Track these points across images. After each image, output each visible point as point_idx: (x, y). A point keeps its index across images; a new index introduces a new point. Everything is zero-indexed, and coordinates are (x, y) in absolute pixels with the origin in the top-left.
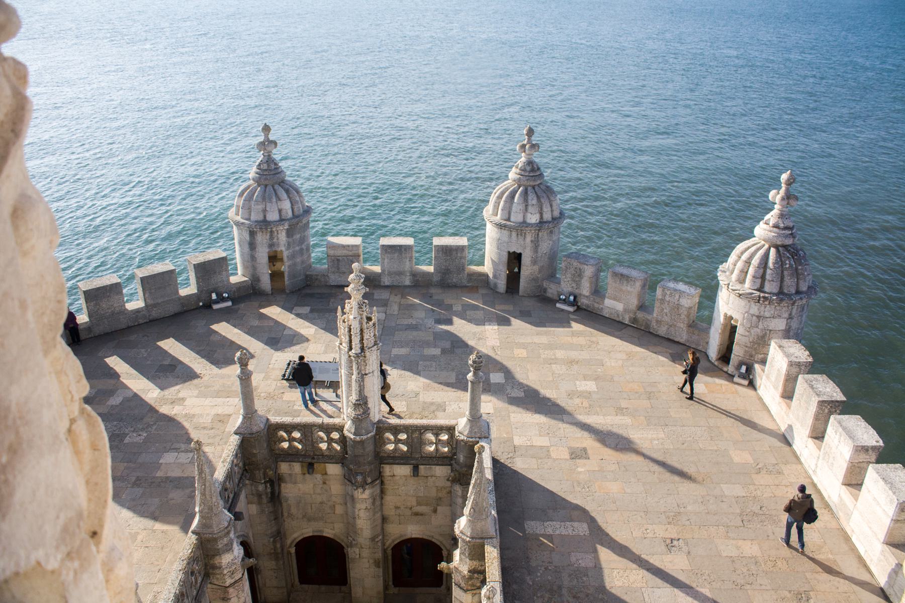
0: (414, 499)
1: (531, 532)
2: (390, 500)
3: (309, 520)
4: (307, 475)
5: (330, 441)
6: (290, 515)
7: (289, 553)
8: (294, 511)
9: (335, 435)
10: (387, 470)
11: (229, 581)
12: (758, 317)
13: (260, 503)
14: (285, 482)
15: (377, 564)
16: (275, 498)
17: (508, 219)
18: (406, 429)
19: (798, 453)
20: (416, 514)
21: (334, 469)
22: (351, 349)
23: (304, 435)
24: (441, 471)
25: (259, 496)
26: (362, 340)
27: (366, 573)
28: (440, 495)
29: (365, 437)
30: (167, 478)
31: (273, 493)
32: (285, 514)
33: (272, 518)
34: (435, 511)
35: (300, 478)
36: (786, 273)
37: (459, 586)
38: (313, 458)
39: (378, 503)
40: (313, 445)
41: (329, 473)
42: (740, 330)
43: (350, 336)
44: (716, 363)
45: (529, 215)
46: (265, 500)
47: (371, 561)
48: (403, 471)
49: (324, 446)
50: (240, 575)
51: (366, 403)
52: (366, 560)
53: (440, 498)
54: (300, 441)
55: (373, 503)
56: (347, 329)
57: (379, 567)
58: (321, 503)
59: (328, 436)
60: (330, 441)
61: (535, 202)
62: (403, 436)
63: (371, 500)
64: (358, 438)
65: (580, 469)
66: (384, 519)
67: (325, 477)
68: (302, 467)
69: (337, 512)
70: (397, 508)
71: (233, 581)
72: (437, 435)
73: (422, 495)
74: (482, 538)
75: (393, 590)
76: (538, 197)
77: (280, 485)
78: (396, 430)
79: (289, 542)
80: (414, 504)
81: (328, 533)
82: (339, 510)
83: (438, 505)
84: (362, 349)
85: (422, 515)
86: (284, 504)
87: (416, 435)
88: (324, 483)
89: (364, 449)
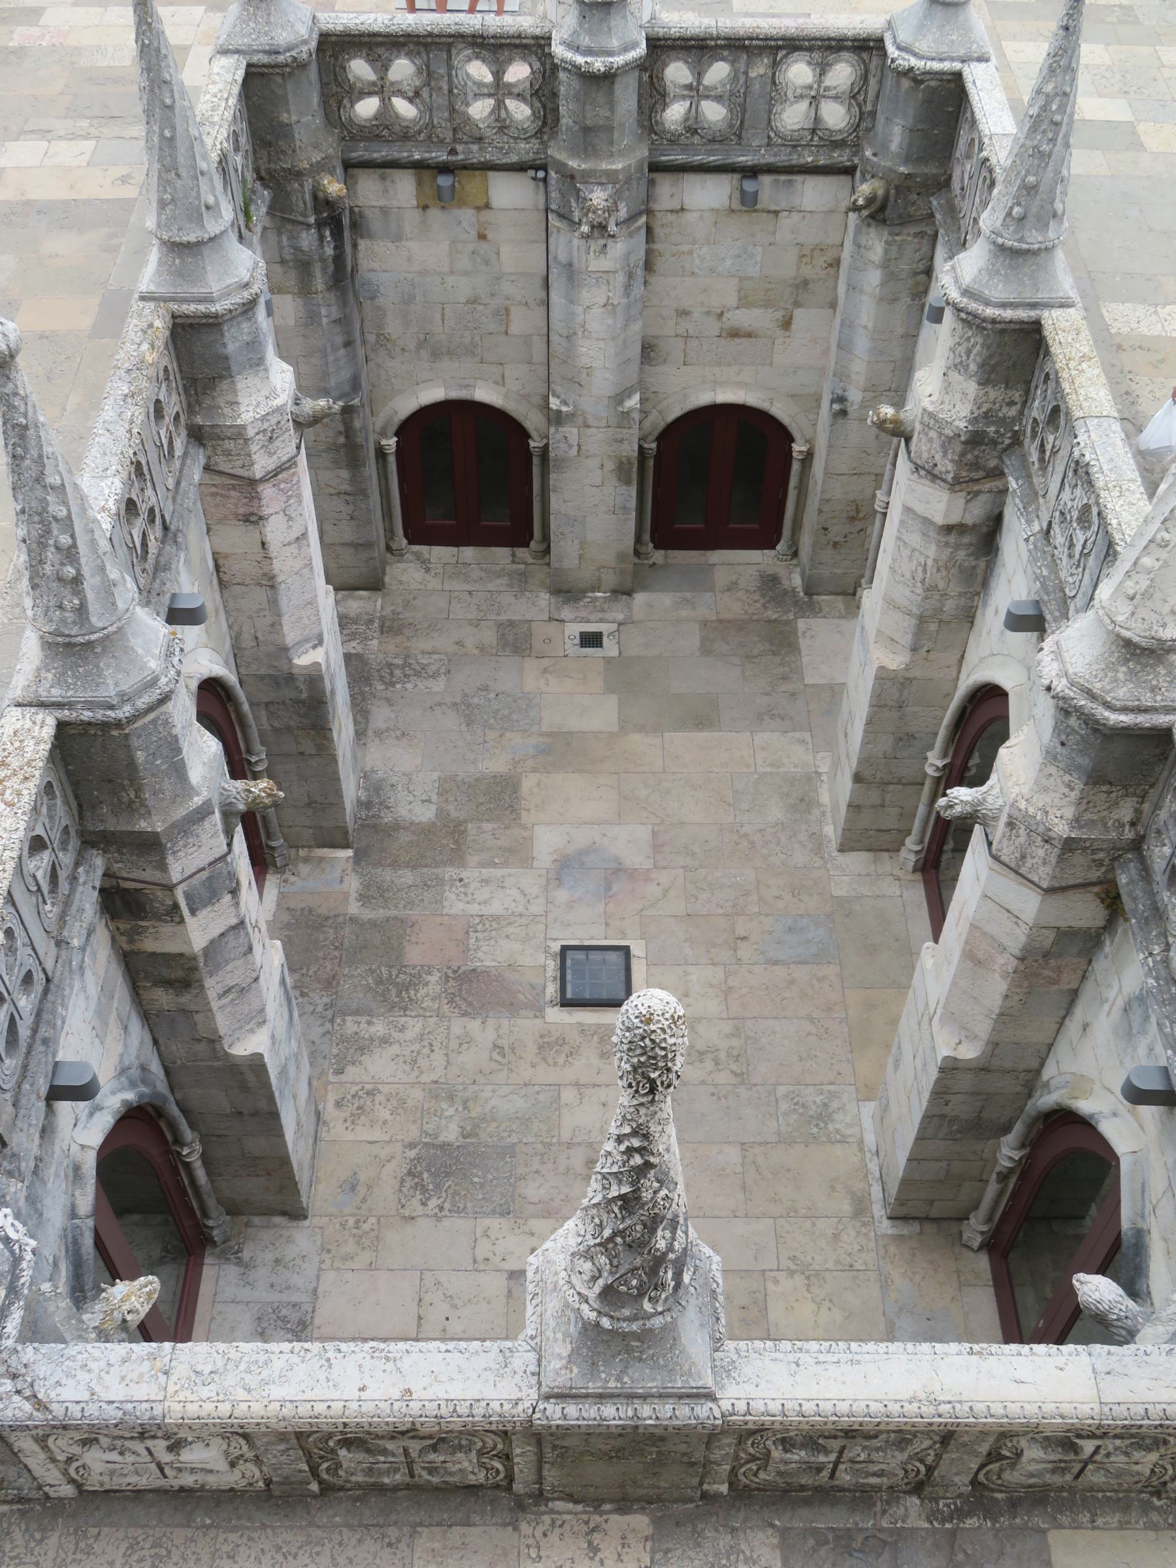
0: (733, 284)
1: (1125, 330)
2: (674, 288)
3: (436, 355)
4: (434, 213)
5: (499, 90)
6: (383, 340)
7: (381, 453)
8: (393, 327)
9: (519, 72)
10: (667, 191)
11: (261, 464)
13: (305, 290)
14: (370, 236)
15: (622, 470)
16: (342, 275)
18: (738, 46)
20: (734, 334)
21: (510, 194)
23: (428, 74)
24: (815, 194)
25: (303, 266)
27: (592, 502)
28: (808, 272)
29: (619, 60)
30: (28, 203)
31: (339, 259)
32: (371, 338)
33: (339, 340)
34: (787, 324)
35: (412, 218)
37: (933, 475)
38: (453, 152)
39: (638, 290)
40: (452, 110)
46: (319, 283)
47: (610, 466)
48: (708, 195)
49: (480, 110)
50: (292, 449)
52: (593, 463)
53: (806, 283)
54: (414, 97)
55: (628, 288)
57: (628, 483)
58: (473, 301)
59: (498, 74)
60: (499, 90)
62: (718, 72)
63: (620, 278)
64: (598, 64)
66: (649, 351)
67: (485, 216)
68: (420, 183)
69: (514, 329)
70: (683, 313)
71: (271, 463)
72: (822, 69)
73: (753, 271)
74: (1033, 306)
75: (658, 556)
77: (355, 246)
78: (699, 48)
79: (379, 422)
80: (732, 300)
81: (485, 394)
83: (797, 304)
85: (749, 335)
86: (367, 306)
87: (760, 68)
88: (482, 237)
89: (611, 104)
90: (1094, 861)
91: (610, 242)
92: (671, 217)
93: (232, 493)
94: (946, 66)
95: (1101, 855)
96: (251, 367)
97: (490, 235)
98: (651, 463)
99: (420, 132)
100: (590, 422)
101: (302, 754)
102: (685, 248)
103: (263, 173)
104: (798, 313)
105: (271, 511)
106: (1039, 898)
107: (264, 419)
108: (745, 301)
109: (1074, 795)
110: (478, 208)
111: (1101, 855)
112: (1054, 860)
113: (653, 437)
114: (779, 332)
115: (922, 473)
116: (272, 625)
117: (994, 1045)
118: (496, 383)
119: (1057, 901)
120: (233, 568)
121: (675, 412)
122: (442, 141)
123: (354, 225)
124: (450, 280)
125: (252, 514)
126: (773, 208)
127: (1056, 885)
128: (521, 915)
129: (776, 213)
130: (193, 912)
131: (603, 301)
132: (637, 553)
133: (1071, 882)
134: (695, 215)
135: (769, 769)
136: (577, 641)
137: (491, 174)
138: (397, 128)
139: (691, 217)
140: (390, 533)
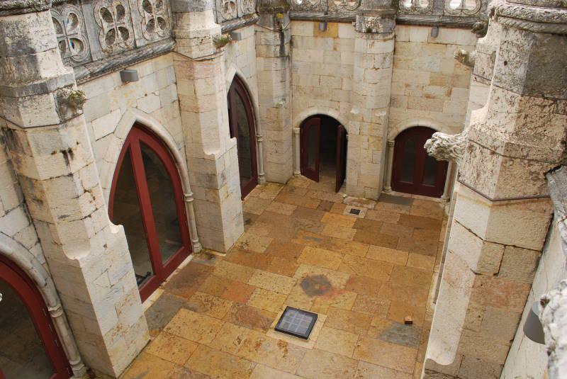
4: (319, 39)
10: (403, 32)
11: (196, 53)
20: (428, 97)
21: (344, 30)
27: (366, 160)
34: (449, 93)
41: (340, 36)
48: (419, 35)
53: (458, 76)
66: (393, 101)
67: (337, 41)
70: (407, 85)
80: (427, 82)
82: (345, 87)
85: (434, 98)
88: (335, 49)
90: (531, 173)
91: (376, 41)
92: (404, 44)
93: (185, 65)
95: (536, 167)
96: (197, 11)
97: (338, 49)
98: (392, 149)
99: (316, 7)
100: (365, 120)
101: (208, 201)
102: (410, 58)
103: (258, 11)
104: (454, 89)
105: (199, 76)
106: (489, 209)
107: (198, 32)
108: (433, 83)
109: (514, 109)
110: (334, 38)
111: (536, 167)
112: (498, 169)
113: (393, 138)
114: (446, 97)
115: (478, 79)
116: (198, 133)
117: (462, 358)
118: (336, 109)
119: (504, 214)
120: (185, 102)
121: (402, 128)
122: (323, 10)
123: (291, 43)
124: (323, 66)
125: (191, 76)
126: (445, 42)
127: (502, 197)
128: (278, 293)
129: (446, 44)
130: (39, 152)
131: (372, 67)
132: (384, 189)
133: (513, 194)
134: (414, 44)
135: (412, 266)
136: (349, 211)
137: (340, 24)
138: (309, 5)
139: (412, 45)
140: (294, 167)
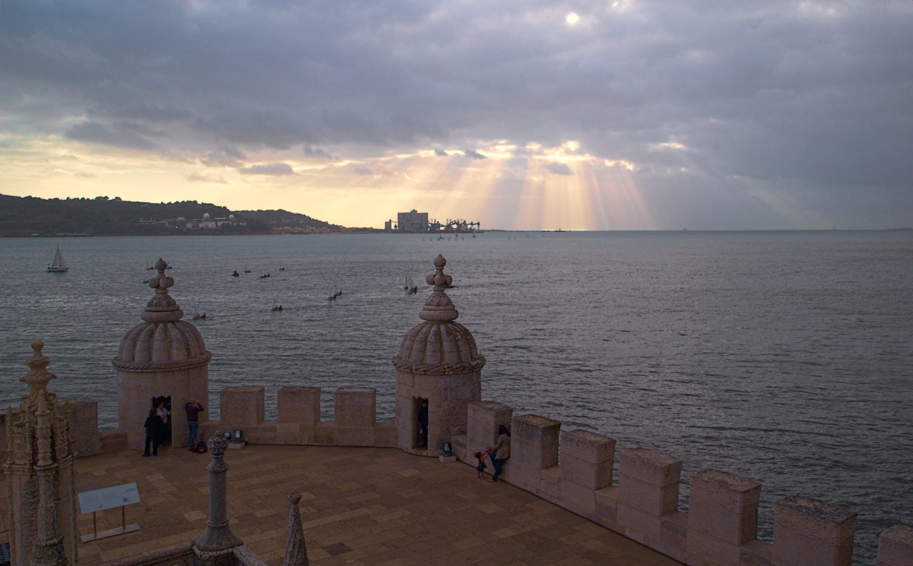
12: (446, 389)
17: (150, 360)
19: (534, 491)
22: (34, 462)
26: (53, 445)
36: (459, 343)
42: (431, 408)
43: (34, 438)
44: (413, 451)
45: (175, 352)
51: (61, 542)
56: (28, 434)
61: (179, 336)
65: (349, 562)
76: (183, 333)
84: (54, 459)
94: (226, 551)
